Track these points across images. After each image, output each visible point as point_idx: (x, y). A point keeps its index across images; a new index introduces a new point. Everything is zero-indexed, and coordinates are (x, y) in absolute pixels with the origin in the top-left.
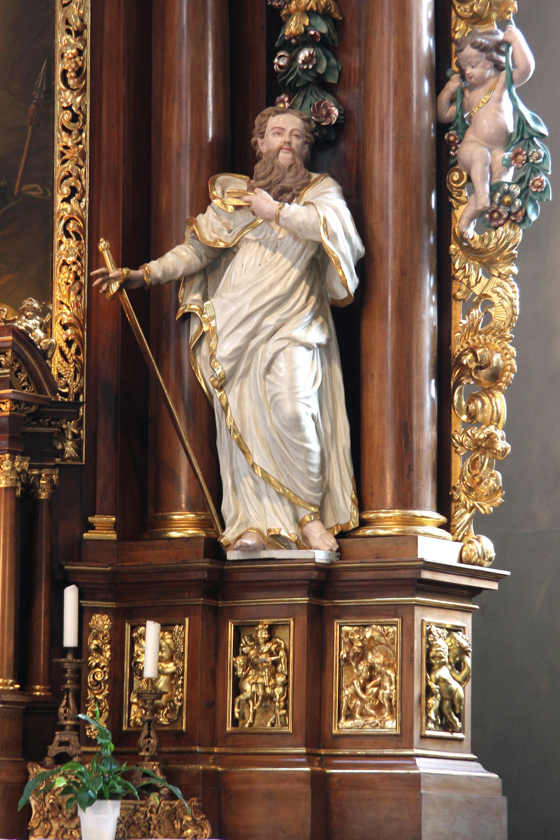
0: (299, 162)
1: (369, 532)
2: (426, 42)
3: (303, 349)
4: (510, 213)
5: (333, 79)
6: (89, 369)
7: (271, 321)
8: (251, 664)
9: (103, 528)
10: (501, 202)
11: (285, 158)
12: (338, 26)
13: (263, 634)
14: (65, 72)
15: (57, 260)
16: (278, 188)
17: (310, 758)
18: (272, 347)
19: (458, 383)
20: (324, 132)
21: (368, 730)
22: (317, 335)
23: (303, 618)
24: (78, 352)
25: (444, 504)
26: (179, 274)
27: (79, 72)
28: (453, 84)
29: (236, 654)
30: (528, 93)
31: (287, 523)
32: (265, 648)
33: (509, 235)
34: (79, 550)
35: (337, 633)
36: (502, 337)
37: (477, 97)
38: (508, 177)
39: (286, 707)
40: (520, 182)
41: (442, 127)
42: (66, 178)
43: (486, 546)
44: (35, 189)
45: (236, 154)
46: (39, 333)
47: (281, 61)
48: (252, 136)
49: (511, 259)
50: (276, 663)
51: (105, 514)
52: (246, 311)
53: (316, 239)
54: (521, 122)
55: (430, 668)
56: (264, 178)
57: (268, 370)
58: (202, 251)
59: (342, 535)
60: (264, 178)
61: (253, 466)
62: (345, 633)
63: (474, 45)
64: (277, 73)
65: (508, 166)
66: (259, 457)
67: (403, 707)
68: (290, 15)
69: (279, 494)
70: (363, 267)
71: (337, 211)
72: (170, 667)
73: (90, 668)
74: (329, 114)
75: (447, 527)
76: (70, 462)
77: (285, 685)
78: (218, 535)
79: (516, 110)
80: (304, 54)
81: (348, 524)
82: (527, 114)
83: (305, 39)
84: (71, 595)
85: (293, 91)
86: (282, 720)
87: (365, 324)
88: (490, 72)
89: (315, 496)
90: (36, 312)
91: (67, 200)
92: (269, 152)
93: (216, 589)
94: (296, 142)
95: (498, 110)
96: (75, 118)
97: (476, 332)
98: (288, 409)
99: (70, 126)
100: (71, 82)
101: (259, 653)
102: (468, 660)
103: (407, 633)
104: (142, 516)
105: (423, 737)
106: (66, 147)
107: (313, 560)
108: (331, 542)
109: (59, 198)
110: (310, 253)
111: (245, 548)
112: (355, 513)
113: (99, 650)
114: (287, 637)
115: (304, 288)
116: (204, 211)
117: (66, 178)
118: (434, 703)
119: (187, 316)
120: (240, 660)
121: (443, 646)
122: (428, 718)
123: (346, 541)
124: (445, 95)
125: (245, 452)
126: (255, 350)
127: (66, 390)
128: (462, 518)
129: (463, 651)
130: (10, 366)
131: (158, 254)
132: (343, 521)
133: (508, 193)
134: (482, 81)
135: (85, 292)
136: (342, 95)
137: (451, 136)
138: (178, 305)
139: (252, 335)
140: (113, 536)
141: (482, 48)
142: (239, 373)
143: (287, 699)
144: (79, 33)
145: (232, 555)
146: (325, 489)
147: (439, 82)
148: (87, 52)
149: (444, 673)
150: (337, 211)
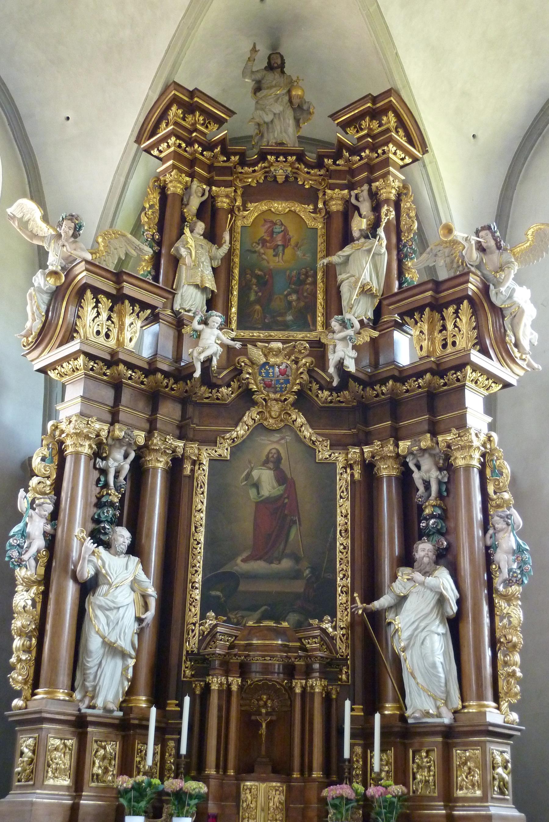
0: (431, 561)
1: (466, 711)
2: (478, 515)
3: (436, 635)
4: (516, 580)
5: (444, 530)
7: (423, 624)
8: (419, 767)
10: (513, 576)
11: (426, 560)
12: (445, 511)
13: (424, 754)
14: (341, 531)
15: (338, 602)
16: (424, 572)
17: (446, 807)
18: (424, 634)
19: (499, 649)
20: (441, 551)
21: (469, 795)
23: (440, 746)
24: (347, 639)
25: (496, 699)
26: (386, 606)
27: (346, 530)
28: (491, 531)
29: (414, 762)
30: (521, 534)
31: (433, 708)
32: (425, 760)
35: (455, 753)
36: (517, 630)
37: (500, 535)
38: (515, 566)
39: (435, 785)
40: (520, 568)
41: (487, 548)
42: (341, 570)
43: (514, 716)
44: (329, 575)
45: (407, 559)
46: (330, 630)
47: (423, 524)
48: (413, 552)
49: (518, 598)
50: (429, 767)
51: (359, 705)
52: (413, 620)
53: (439, 591)
54: (519, 545)
55: (494, 768)
56: (418, 568)
57: (422, 643)
58: (394, 597)
59: (455, 712)
60: (418, 568)
61: (418, 683)
63: (498, 516)
64: (422, 529)
65: (515, 562)
66: (420, 680)
67: (484, 786)
68: (426, 507)
69: (428, 695)
70: (459, 602)
71: (447, 580)
72: (386, 768)
73: (354, 769)
74: (443, 544)
75: (498, 708)
76: (344, 683)
77: (434, 776)
78: (404, 713)
79: (516, 540)
80: (432, 521)
81: (457, 708)
82: (521, 542)
83: (432, 516)
85: (428, 536)
87: (461, 625)
88: (505, 526)
89: (443, 696)
90: (329, 622)
91: (342, 579)
92: (420, 558)
93: (404, 735)
94: (430, 554)
95: (509, 541)
96: (345, 548)
97: (506, 628)
98: (431, 659)
99: (343, 551)
100: (343, 534)
101: (423, 762)
102: (509, 765)
103: (484, 753)
105: (492, 798)
106: (341, 559)
107: (443, 722)
108: (451, 716)
109: (339, 579)
110: (437, 597)
111: (415, 718)
112: (460, 703)
113: (357, 761)
114: (434, 756)
115: (435, 611)
116: (395, 582)
117: (341, 570)
118: (496, 783)
119: (390, 624)
120: (415, 766)
121: (499, 759)
122: (494, 790)
123: (457, 715)
124: (488, 535)
125: (414, 678)
126: (417, 636)
127: (342, 654)
128: (505, 706)
129: (507, 762)
130: (319, 643)
131: (378, 598)
132: (455, 706)
133: (515, 572)
134: (502, 530)
135: (349, 615)
136: (448, 537)
137: (491, 551)
138: (386, 619)
139: (416, 629)
140: (362, 714)
141: (501, 517)
142: (411, 645)
143: (435, 782)
144: (346, 516)
145: (410, 721)
147: (485, 531)
148: (349, 523)
149: (500, 770)
150: (447, 580)
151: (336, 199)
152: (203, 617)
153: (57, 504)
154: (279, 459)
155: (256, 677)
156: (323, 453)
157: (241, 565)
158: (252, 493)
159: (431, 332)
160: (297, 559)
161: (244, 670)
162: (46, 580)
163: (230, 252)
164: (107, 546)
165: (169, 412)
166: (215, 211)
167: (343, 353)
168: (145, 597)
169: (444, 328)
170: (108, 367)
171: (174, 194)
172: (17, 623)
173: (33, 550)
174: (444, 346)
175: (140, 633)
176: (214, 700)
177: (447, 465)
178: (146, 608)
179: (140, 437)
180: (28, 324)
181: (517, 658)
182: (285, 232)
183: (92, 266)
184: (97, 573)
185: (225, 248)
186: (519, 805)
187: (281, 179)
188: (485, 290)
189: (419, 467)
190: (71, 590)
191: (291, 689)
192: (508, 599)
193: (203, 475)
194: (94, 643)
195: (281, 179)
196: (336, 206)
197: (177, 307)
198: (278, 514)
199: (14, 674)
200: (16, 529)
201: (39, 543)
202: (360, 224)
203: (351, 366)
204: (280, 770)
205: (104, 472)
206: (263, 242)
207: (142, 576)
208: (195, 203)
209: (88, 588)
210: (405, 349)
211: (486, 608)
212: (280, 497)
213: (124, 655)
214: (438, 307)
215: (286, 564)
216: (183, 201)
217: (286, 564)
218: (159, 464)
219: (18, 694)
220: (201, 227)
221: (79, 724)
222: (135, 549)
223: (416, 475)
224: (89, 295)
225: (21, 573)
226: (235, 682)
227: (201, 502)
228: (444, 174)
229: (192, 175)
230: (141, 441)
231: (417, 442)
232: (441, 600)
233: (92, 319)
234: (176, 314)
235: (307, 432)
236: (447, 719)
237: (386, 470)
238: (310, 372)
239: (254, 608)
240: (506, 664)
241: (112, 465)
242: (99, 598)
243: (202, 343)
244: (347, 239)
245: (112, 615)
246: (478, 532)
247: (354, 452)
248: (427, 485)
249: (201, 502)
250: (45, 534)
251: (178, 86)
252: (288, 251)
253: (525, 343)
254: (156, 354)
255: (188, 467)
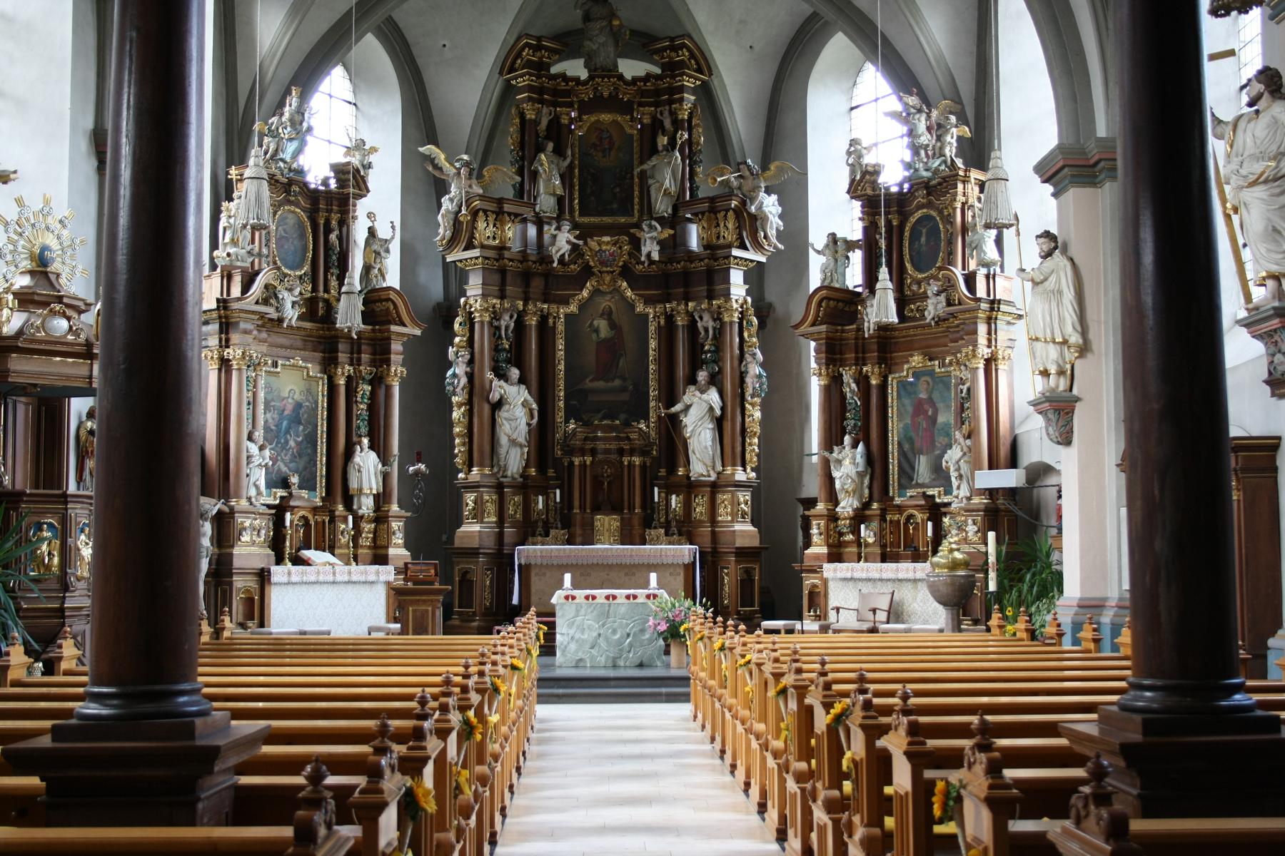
6: (659, 433)
9: (663, 472)
22: (711, 426)
25: (744, 465)
30: (762, 365)
33: (758, 400)
34: (657, 478)
41: (742, 373)
43: (753, 475)
45: (692, 381)
59: (719, 473)
62: (720, 497)
67: (732, 515)
70: (723, 409)
75: (745, 470)
83: (709, 351)
84: (656, 489)
86: (704, 518)
93: (689, 487)
95: (755, 369)
104: (672, 469)
128: (749, 470)
146: (714, 462)
151: (645, 115)
152: (567, 421)
153: (472, 354)
154: (610, 312)
155: (600, 457)
156: (640, 308)
157: (589, 384)
158: (594, 336)
159: (709, 228)
160: (624, 379)
161: (593, 452)
162: (470, 402)
163: (572, 162)
164: (506, 381)
165: (537, 284)
166: (559, 123)
167: (651, 249)
168: (531, 410)
169: (718, 225)
170: (497, 255)
171: (530, 120)
172: (457, 430)
173: (462, 384)
174: (718, 238)
175: (529, 432)
176: (577, 471)
177: (717, 317)
178: (532, 417)
179: (520, 304)
180: (441, 231)
181: (756, 440)
182: (611, 137)
183: (482, 197)
184: (502, 397)
185: (568, 160)
186: (753, 523)
187: (606, 94)
188: (744, 203)
189: (701, 318)
190: (487, 408)
191: (622, 463)
192: (753, 405)
193: (561, 327)
194: (504, 440)
195: (606, 94)
196: (647, 120)
197: (537, 209)
198: (611, 348)
199: (457, 460)
200: (450, 373)
201: (464, 380)
202: (663, 141)
203: (655, 256)
204: (615, 508)
205: (498, 328)
206: (594, 145)
207: (529, 398)
208: (544, 122)
209: (498, 405)
210: (694, 237)
211: (738, 411)
212: (611, 339)
213: (521, 446)
214: (713, 210)
215: (617, 382)
216: (536, 122)
217: (617, 382)
218: (533, 321)
219: (461, 471)
220: (550, 146)
221: (499, 488)
222: (522, 381)
223: (699, 324)
224: (481, 213)
225: (455, 399)
226: (589, 460)
227: (561, 345)
228: (727, 81)
229: (541, 102)
230: (521, 308)
231: (700, 304)
232: (711, 409)
233: (484, 230)
234: (537, 214)
235: (629, 293)
236: (713, 477)
237: (680, 321)
238: (630, 254)
239: (599, 411)
240: (750, 444)
241: (503, 323)
242: (503, 414)
243: (557, 243)
244: (654, 151)
245: (513, 424)
246: (736, 363)
247: (659, 308)
248: (706, 330)
249: (561, 345)
250: (466, 373)
251: (528, 36)
252: (613, 153)
253: (772, 233)
254: (526, 246)
255: (551, 321)
